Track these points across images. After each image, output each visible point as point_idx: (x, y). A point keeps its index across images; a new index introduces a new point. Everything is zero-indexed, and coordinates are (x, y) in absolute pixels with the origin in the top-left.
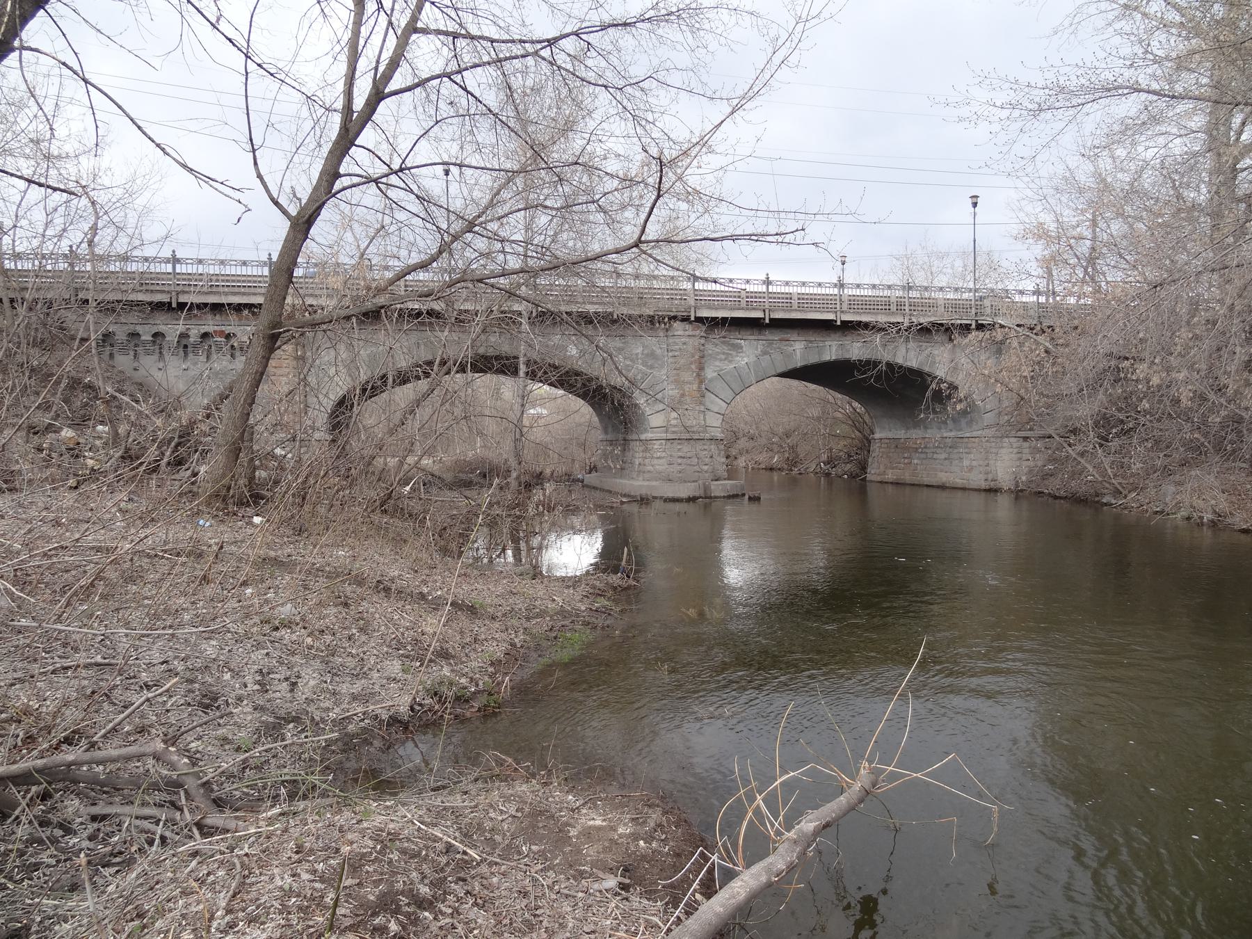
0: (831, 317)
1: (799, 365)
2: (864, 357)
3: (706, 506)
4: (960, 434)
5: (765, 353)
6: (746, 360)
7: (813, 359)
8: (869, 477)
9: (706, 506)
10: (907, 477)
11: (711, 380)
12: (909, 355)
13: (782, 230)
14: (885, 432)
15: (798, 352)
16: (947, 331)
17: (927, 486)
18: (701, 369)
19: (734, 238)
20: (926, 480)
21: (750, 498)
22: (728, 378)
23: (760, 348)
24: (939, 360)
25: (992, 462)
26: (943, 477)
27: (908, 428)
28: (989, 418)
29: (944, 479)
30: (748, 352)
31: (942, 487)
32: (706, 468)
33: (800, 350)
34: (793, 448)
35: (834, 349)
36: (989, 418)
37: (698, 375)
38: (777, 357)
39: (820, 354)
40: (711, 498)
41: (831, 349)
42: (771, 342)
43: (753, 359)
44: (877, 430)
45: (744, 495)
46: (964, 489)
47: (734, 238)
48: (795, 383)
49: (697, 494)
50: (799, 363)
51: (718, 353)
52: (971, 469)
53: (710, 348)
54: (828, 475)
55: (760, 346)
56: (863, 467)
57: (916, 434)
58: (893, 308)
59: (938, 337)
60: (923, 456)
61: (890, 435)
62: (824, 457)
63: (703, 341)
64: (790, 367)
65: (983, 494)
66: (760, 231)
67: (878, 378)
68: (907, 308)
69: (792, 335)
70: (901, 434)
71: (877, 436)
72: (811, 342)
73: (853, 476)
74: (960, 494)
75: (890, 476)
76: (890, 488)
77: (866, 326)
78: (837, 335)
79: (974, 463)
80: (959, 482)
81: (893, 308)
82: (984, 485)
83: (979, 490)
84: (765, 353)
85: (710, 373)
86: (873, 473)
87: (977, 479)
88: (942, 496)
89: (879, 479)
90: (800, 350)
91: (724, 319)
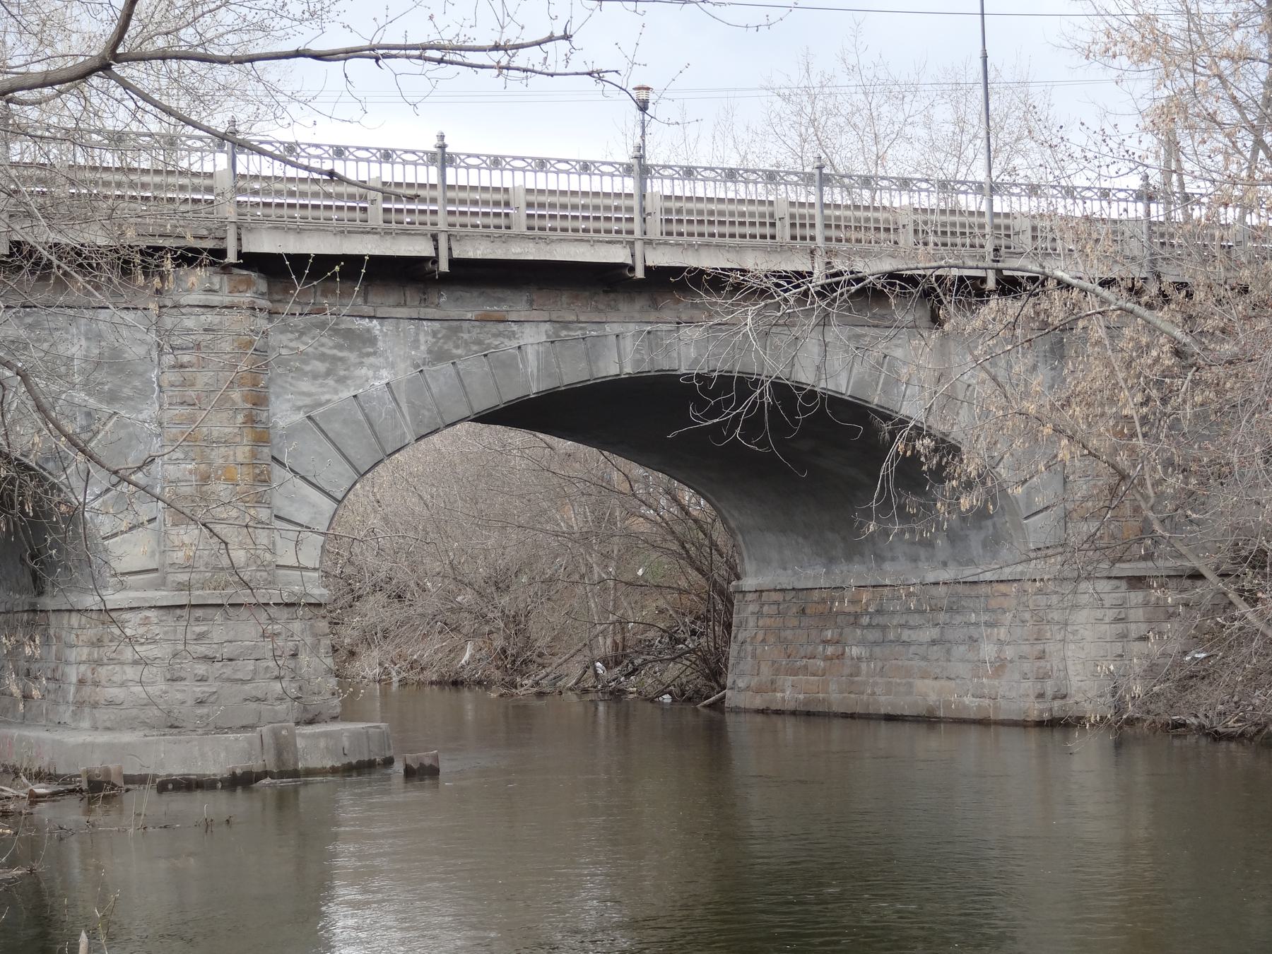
0: (618, 255)
1: (535, 388)
3: (283, 800)
4: (968, 573)
5: (439, 356)
6: (386, 375)
7: (573, 373)
8: (733, 698)
9: (283, 800)
10: (835, 696)
11: (291, 432)
12: (827, 360)
13: (512, 35)
14: (771, 570)
15: (531, 353)
16: (923, 296)
17: (889, 718)
18: (260, 401)
19: (377, 53)
20: (885, 703)
21: (410, 773)
22: (334, 427)
23: (425, 341)
24: (904, 374)
25: (1050, 647)
26: (928, 693)
27: (831, 560)
28: (1039, 529)
29: (932, 698)
30: (393, 354)
31: (929, 720)
32: (277, 686)
33: (537, 348)
34: (516, 622)
35: (628, 345)
36: (1039, 529)
37: (251, 420)
38: (473, 367)
39: (591, 356)
40: (295, 774)
41: (622, 346)
42: (454, 326)
43: (404, 372)
44: (749, 566)
45: (389, 762)
46: (984, 723)
47: (377, 53)
48: (517, 437)
49: (256, 765)
50: (532, 378)
51: (304, 357)
52: (1000, 666)
53: (283, 343)
54: (617, 695)
55: (425, 335)
56: (714, 670)
57: (853, 574)
58: (783, 232)
59: (905, 313)
60: (873, 635)
61: (785, 579)
62: (605, 646)
63: (262, 323)
64: (512, 393)
65: (1034, 734)
66: (447, 36)
67: (753, 425)
68: (819, 232)
69: (516, 306)
70: (813, 575)
71: (749, 583)
72: (566, 324)
73: (685, 697)
74: (973, 734)
75: (789, 694)
76: (789, 730)
77: (715, 282)
78: (641, 303)
79: (1009, 652)
80: (971, 704)
81: (783, 232)
82: (1035, 710)
83: (1023, 724)
84: (439, 356)
85: (284, 413)
86: (742, 687)
87: (1017, 696)
88: (931, 744)
89: (758, 702)
90: (537, 348)
91: (323, 264)
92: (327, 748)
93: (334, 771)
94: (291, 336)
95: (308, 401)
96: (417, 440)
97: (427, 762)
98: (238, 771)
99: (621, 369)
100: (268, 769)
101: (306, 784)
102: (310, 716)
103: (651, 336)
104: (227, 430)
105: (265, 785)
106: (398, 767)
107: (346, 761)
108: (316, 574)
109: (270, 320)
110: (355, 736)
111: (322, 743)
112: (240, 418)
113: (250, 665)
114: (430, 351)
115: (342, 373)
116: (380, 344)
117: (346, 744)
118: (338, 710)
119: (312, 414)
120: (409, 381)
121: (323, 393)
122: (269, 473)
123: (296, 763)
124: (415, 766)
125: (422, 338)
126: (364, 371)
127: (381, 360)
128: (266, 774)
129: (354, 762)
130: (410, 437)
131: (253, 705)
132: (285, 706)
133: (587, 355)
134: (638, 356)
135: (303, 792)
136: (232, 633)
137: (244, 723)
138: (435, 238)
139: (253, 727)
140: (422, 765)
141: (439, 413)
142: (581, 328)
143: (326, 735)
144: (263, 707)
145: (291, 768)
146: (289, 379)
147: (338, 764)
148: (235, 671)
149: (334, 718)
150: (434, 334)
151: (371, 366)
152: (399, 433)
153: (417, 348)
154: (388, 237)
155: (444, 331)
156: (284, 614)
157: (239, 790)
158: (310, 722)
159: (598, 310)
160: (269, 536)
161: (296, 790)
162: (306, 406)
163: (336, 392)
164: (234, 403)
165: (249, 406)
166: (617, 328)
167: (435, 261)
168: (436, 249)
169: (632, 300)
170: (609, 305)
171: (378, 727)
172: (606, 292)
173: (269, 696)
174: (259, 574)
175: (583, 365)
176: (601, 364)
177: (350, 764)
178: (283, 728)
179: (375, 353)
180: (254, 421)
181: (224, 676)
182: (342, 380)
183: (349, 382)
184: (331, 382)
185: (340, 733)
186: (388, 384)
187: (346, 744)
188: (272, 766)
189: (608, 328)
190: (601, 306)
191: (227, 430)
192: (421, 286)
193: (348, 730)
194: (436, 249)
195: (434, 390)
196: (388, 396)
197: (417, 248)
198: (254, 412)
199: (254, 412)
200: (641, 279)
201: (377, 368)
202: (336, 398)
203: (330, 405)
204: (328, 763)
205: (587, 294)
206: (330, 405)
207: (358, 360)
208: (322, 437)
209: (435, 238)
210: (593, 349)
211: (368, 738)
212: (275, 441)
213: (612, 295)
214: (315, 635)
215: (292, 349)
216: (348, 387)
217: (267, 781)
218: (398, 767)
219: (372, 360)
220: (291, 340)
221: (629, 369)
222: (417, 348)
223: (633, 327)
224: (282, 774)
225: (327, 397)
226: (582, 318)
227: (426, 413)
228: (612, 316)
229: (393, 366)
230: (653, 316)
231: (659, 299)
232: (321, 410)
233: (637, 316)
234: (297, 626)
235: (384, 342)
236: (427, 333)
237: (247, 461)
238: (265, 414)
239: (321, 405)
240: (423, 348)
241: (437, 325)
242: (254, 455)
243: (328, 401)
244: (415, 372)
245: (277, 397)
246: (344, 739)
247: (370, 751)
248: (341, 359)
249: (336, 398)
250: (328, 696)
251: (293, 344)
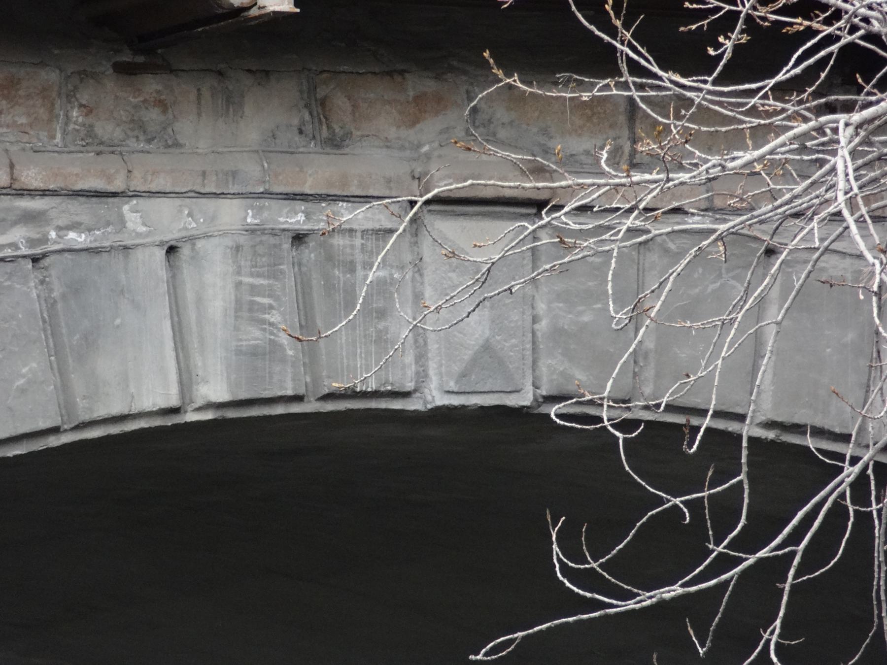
2: (763, 406)
35: (215, 282)
39: (67, 337)
99: (186, 384)
103: (310, 253)
133: (51, 324)
134: (254, 335)
142: (29, 218)
159: (91, 141)
166: (170, 219)
169: (231, 104)
170: (138, 126)
172: (125, 70)
175: (32, 366)
176: (106, 366)
189: (133, 217)
190: (106, 129)
200: (278, 17)
205: (51, 76)
210: (72, 303)
213: (152, 85)
221: (215, 388)
223: (233, 214)
226: (31, 177)
228: (152, 168)
230: (318, 171)
231: (340, 102)
233: (252, 171)
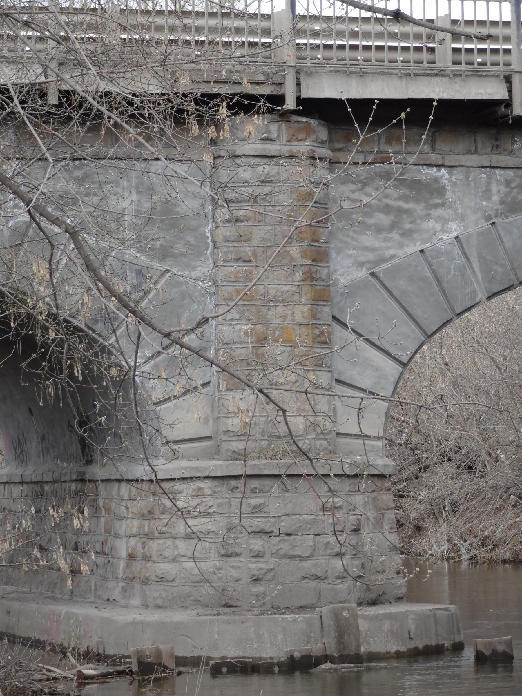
6: (455, 228)
18: (319, 256)
21: (481, 659)
22: (400, 285)
23: (498, 191)
32: (338, 564)
37: (310, 277)
40: (357, 658)
43: (475, 225)
49: (315, 648)
51: (367, 210)
53: (345, 194)
55: (498, 185)
63: (322, 172)
85: (345, 270)
91: (389, 108)
92: (392, 632)
93: (399, 655)
94: (353, 187)
95: (370, 256)
96: (489, 298)
97: (500, 648)
98: (297, 655)
100: (328, 653)
101: (369, 669)
102: (374, 596)
104: (285, 288)
105: (326, 671)
106: (469, 655)
107: (411, 645)
108: (379, 443)
109: (331, 170)
110: (422, 618)
111: (386, 626)
112: (299, 275)
113: (310, 540)
114: (502, 202)
115: (408, 226)
116: (449, 195)
117: (412, 627)
118: (404, 590)
119: (375, 270)
120: (481, 234)
121: (388, 248)
122: (330, 334)
123: (358, 647)
124: (487, 652)
125: (494, 188)
126: (431, 224)
127: (450, 212)
128: (326, 658)
129: (421, 646)
130: (481, 295)
131: (312, 584)
132: (346, 585)
135: (365, 678)
136: (290, 506)
137: (303, 603)
138: (508, 79)
139: (312, 607)
140: (494, 651)
141: (514, 269)
143: (391, 617)
144: (322, 585)
145: (352, 651)
146: (351, 233)
147: (403, 649)
148: (294, 547)
149: (399, 599)
150: (508, 183)
151: (439, 219)
152: (469, 290)
153: (488, 198)
154: (457, 79)
155: (518, 180)
156: (346, 485)
157: (297, 674)
158: (374, 603)
160: (329, 403)
161: (358, 675)
162: (369, 262)
163: (401, 246)
164: (293, 259)
165: (309, 262)
167: (508, 104)
168: (510, 91)
171: (446, 609)
173: (329, 574)
174: (318, 442)
177: (416, 649)
178: (343, 609)
179: (443, 205)
180: (313, 279)
181: (282, 552)
182: (407, 234)
183: (415, 236)
184: (395, 236)
185: (405, 615)
186: (457, 238)
187: (412, 627)
188: (332, 650)
191: (285, 288)
192: (494, 131)
193: (414, 612)
194: (510, 91)
195: (508, 244)
196: (457, 250)
197: (489, 91)
198: (313, 269)
199: (313, 269)
201: (445, 221)
202: (400, 253)
203: (395, 261)
204: (393, 648)
206: (395, 261)
207: (424, 213)
208: (386, 295)
209: (508, 79)
211: (436, 621)
212: (335, 300)
214: (378, 509)
215: (354, 201)
216: (414, 241)
217: (327, 666)
218: (469, 655)
219: (440, 212)
220: (353, 192)
222: (488, 198)
224: (343, 659)
225: (392, 252)
227: (499, 269)
229: (462, 218)
232: (385, 266)
234: (358, 499)
235: (454, 192)
236: (499, 182)
237: (306, 321)
238: (326, 271)
239: (384, 260)
240: (495, 198)
241: (510, 173)
242: (314, 315)
243: (393, 257)
244: (484, 225)
245: (338, 253)
246: (410, 622)
247: (438, 635)
248: (407, 211)
249: (400, 253)
250: (393, 575)
251: (355, 196)
